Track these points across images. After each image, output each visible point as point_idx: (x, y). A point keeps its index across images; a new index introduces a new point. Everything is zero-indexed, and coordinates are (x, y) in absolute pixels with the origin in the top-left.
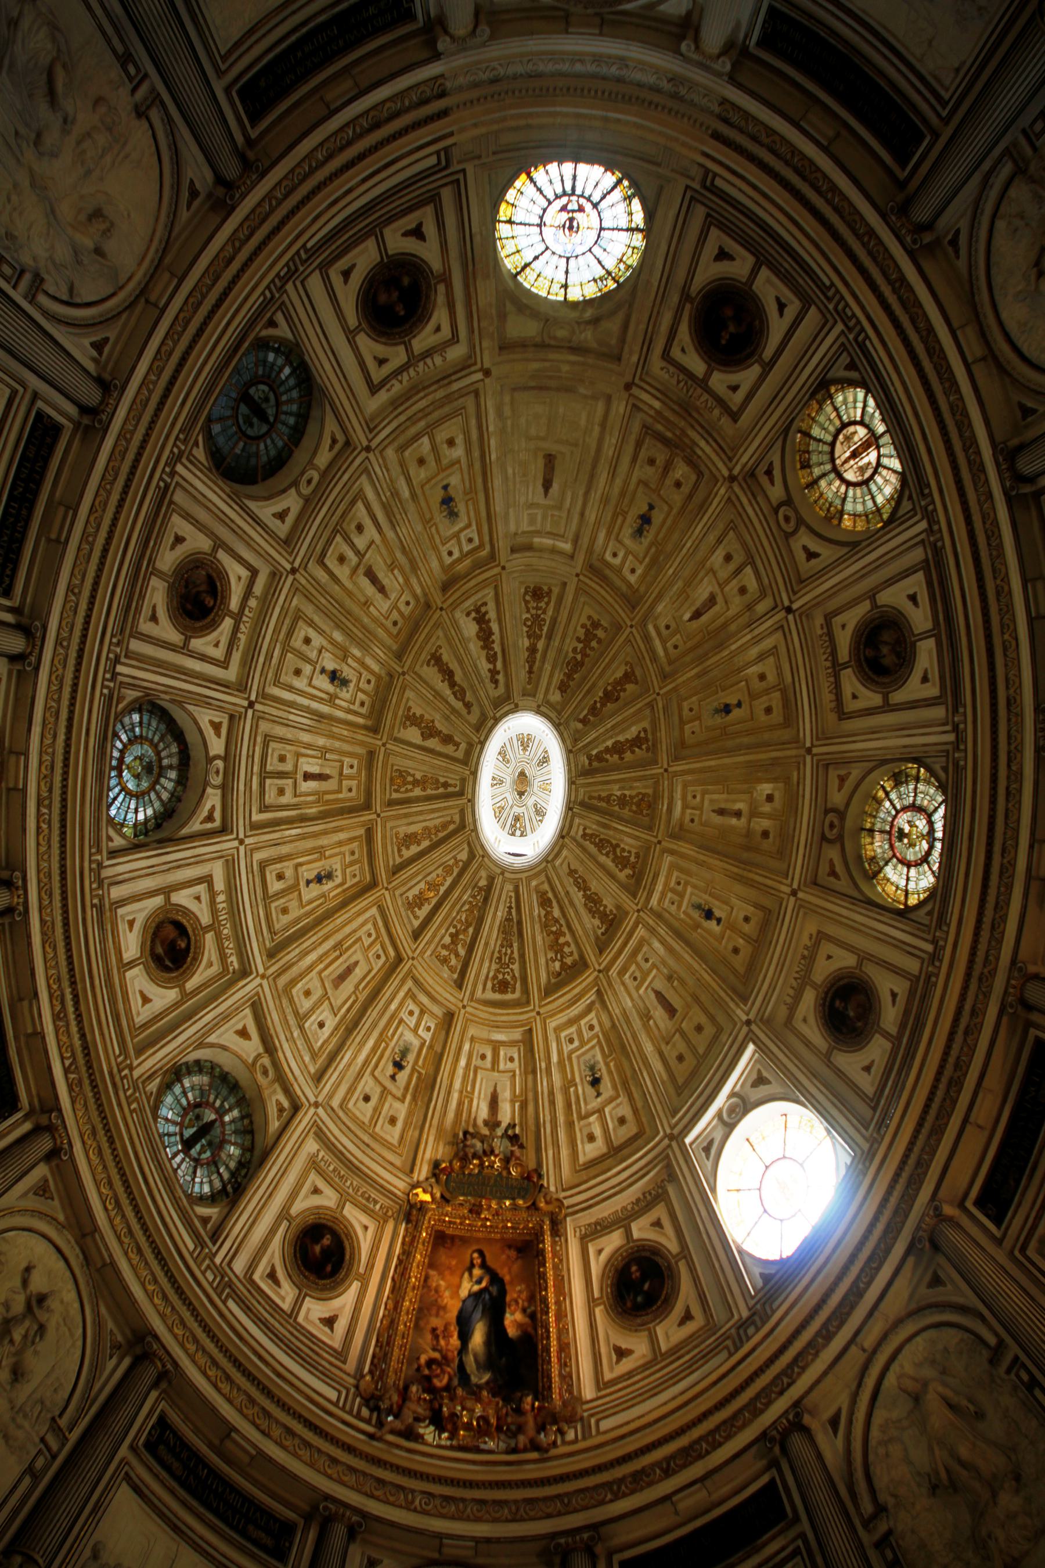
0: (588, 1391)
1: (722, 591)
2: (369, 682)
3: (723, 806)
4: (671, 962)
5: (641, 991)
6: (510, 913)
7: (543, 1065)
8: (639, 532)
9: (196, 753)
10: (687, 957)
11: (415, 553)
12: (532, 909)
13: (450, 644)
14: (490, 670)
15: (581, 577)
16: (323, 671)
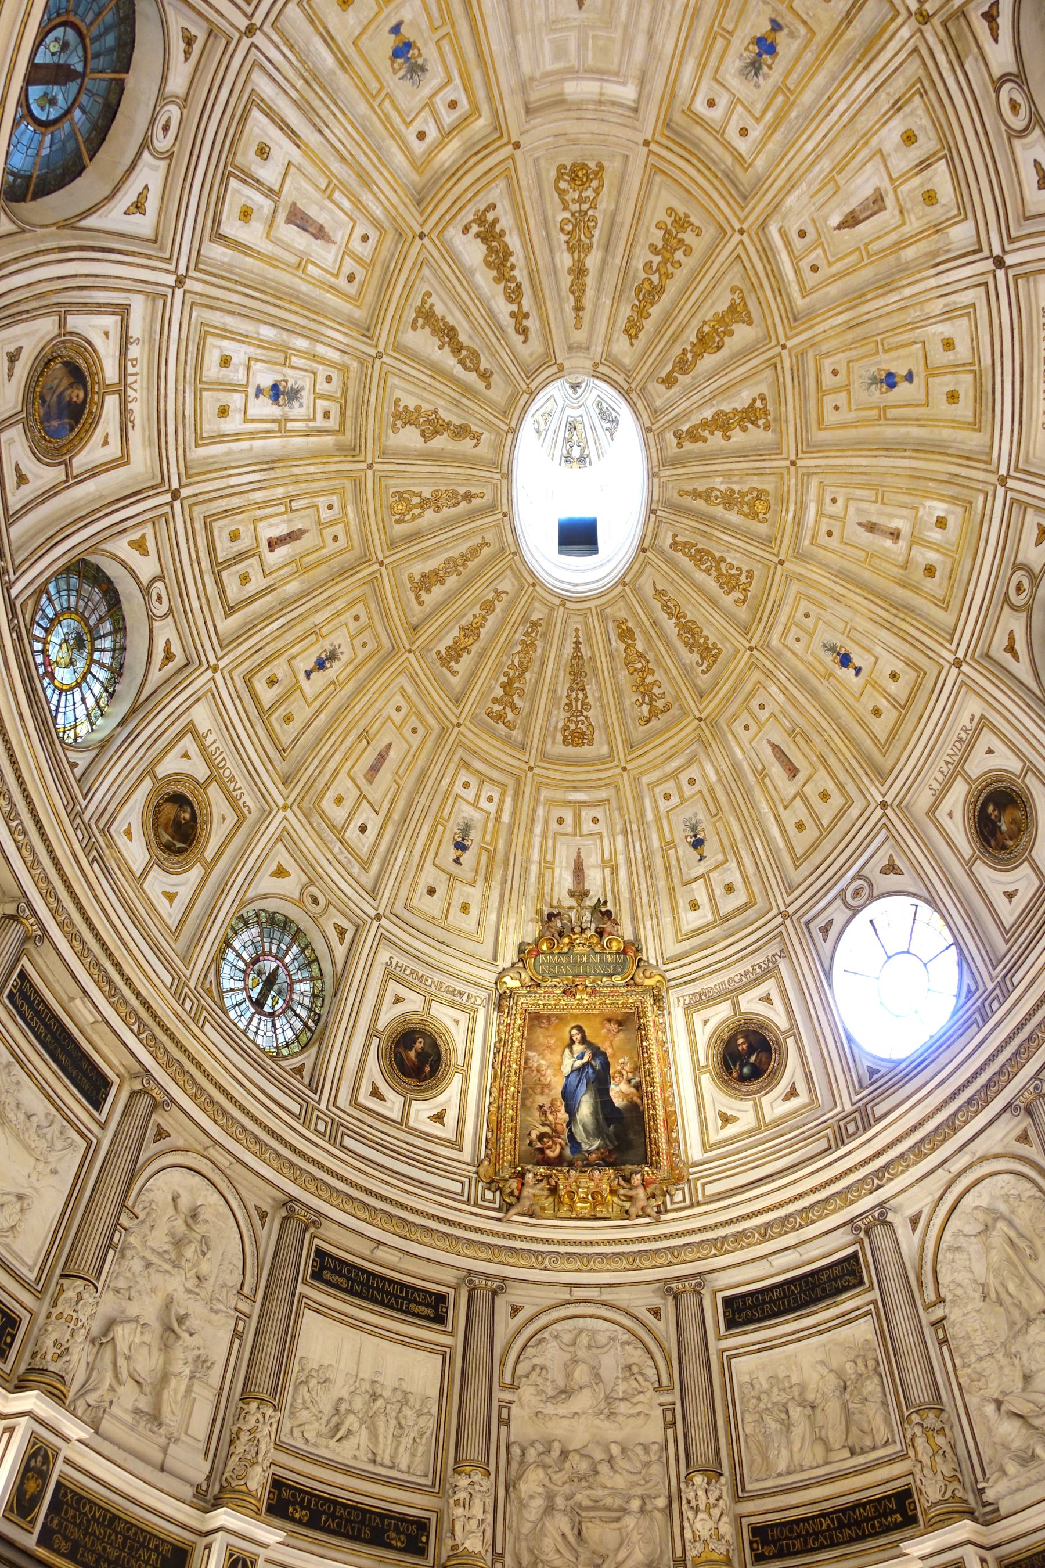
0: (694, 1152)
1: (895, 191)
2: (329, 379)
3: (874, 519)
4: (792, 711)
7: (635, 827)
8: (755, 67)
9: (126, 587)
11: (363, 160)
13: (444, 287)
14: (512, 314)
15: (653, 147)
16: (259, 391)
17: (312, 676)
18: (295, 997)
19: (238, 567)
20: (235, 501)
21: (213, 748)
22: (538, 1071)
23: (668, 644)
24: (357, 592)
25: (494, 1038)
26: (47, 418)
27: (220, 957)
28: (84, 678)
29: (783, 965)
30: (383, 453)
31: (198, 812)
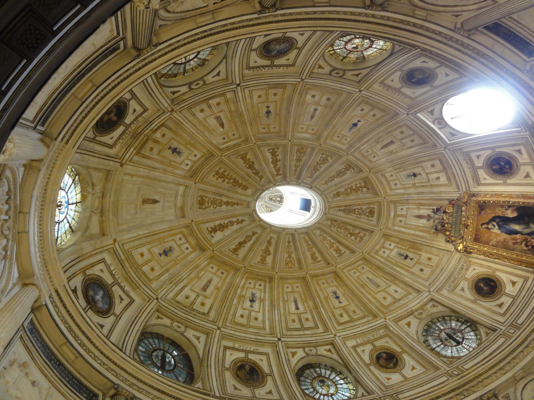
2: (250, 283)
4: (371, 141)
5: (380, 154)
6: (341, 210)
7: (406, 196)
8: (179, 153)
10: (371, 136)
11: (192, 267)
12: (341, 201)
14: (237, 224)
15: (196, 181)
16: (251, 306)
17: (341, 301)
18: (457, 328)
19: (303, 321)
20: (283, 319)
21: (362, 340)
22: (498, 242)
23: (343, 181)
24: (315, 282)
25: (482, 257)
26: (253, 379)
27: (438, 354)
28: (334, 382)
29: (465, 150)
30: (273, 268)
31: (384, 351)
